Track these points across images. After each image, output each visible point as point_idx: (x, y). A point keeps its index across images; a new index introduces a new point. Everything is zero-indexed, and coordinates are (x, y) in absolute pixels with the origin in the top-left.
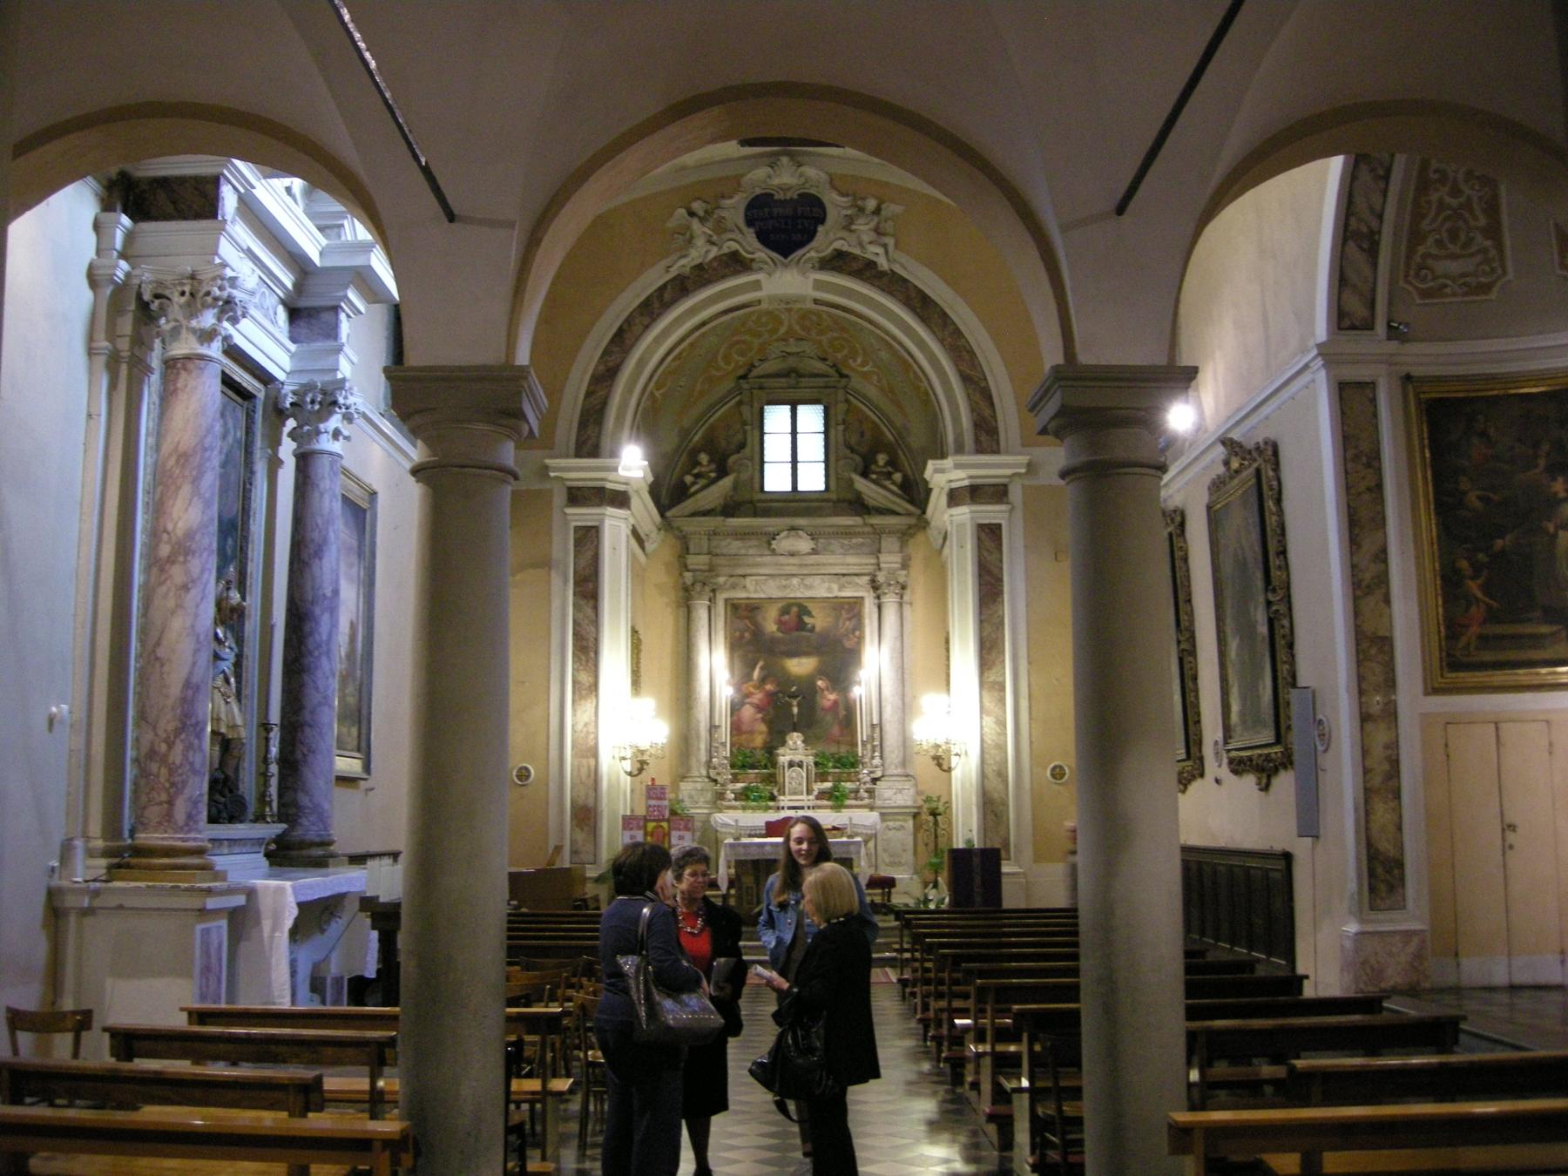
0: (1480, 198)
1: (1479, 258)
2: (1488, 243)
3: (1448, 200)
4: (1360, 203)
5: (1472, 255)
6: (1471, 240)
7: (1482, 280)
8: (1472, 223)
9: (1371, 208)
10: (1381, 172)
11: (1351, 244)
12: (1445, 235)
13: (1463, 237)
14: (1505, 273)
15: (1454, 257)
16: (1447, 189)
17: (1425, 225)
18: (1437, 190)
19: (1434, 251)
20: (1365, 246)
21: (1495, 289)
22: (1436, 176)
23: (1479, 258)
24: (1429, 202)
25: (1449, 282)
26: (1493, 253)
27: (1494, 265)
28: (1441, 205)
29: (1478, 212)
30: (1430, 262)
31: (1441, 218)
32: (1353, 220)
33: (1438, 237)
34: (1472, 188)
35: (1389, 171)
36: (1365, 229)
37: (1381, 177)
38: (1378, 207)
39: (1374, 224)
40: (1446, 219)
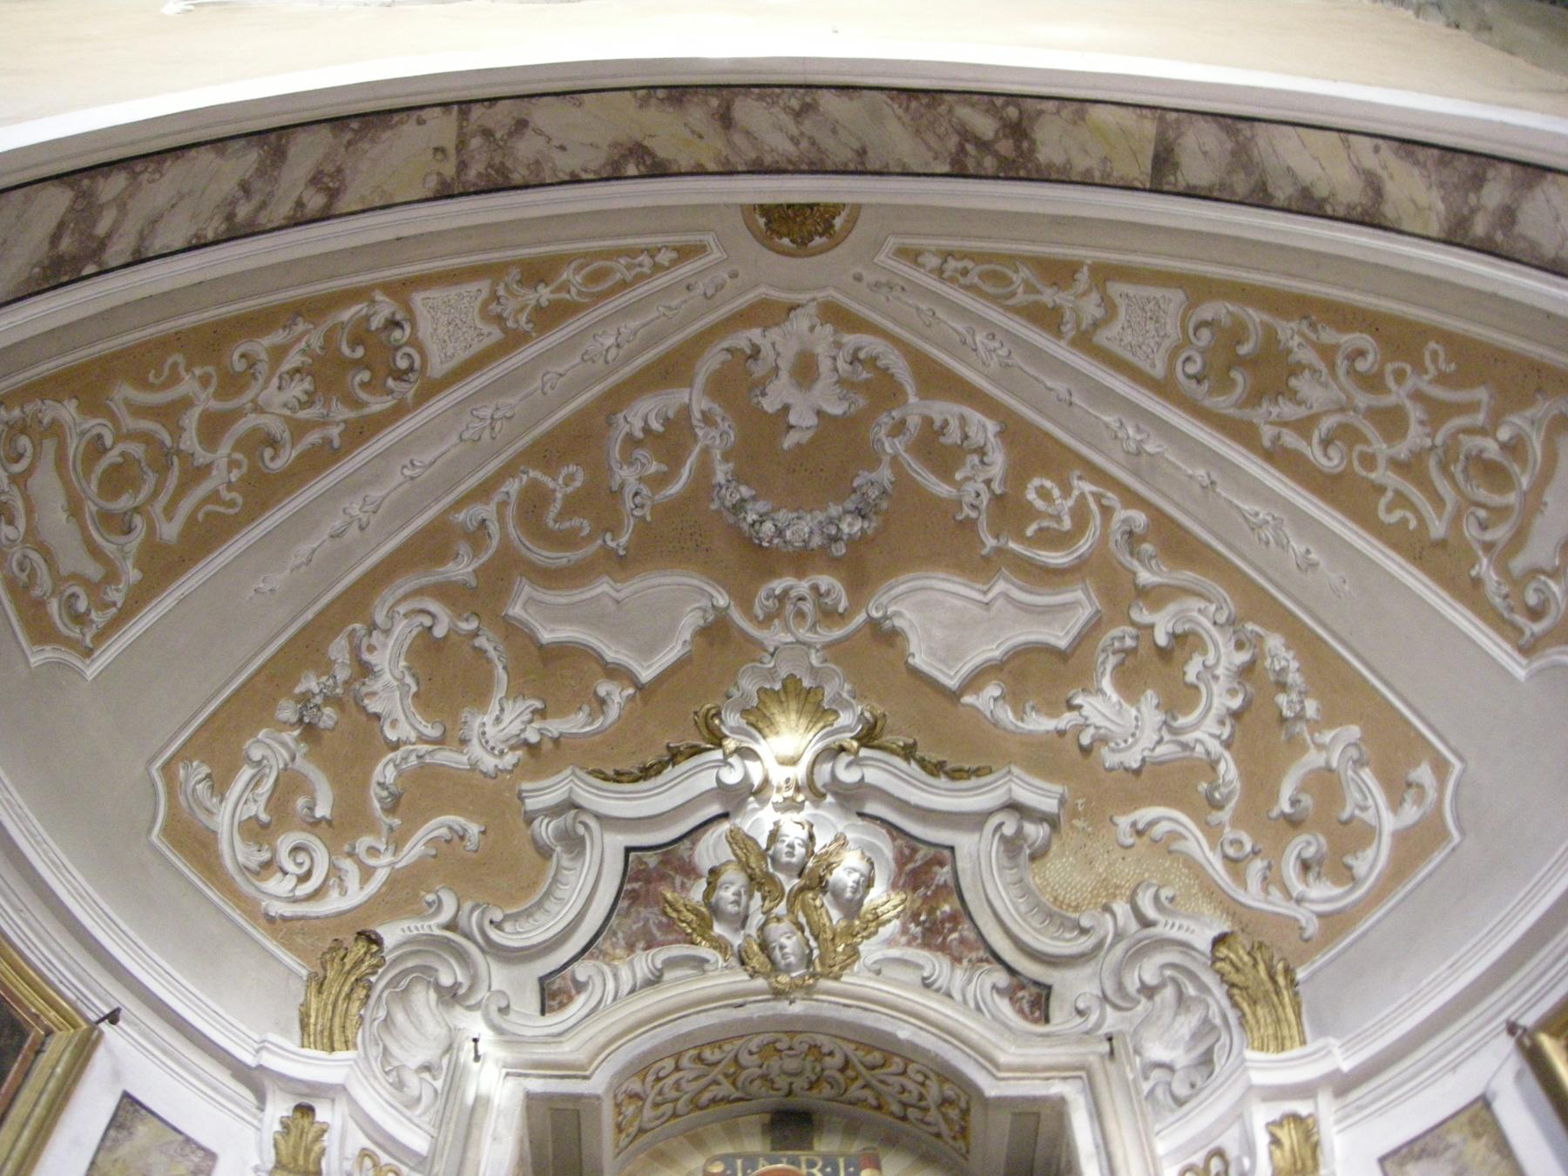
0: (214, 497)
1: (93, 571)
2: (133, 575)
3: (191, 420)
4: (159, 189)
5: (95, 552)
6: (119, 524)
7: (54, 606)
8: (158, 507)
9: (154, 221)
10: (243, 211)
11: (58, 200)
12: (113, 457)
13: (124, 502)
14: (88, 653)
15: (75, 509)
16: (215, 405)
17: (124, 392)
18: (205, 381)
19: (74, 446)
20: (66, 245)
21: (49, 653)
22: (239, 366)
23: (93, 571)
24: (174, 379)
25: (21, 523)
26: (117, 595)
27: (94, 615)
28: (170, 414)
29: (186, 507)
30: (49, 446)
31: (146, 425)
32: (119, 181)
33: (108, 441)
34: (233, 464)
35: (251, 231)
36: (102, 228)
37: (230, 217)
38: (157, 245)
39: (118, 250)
40: (147, 438)
